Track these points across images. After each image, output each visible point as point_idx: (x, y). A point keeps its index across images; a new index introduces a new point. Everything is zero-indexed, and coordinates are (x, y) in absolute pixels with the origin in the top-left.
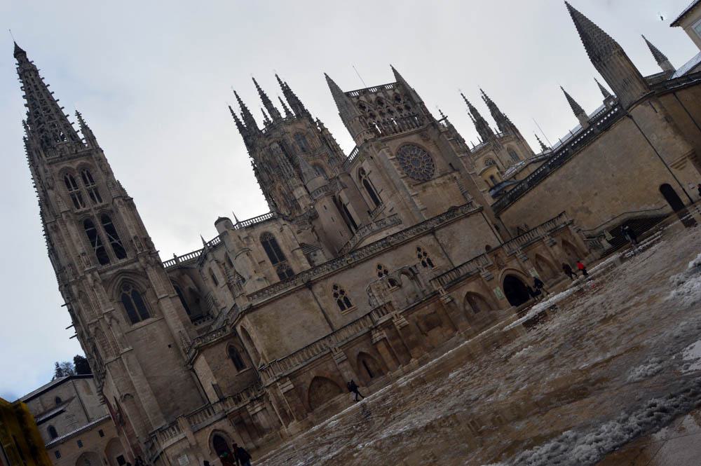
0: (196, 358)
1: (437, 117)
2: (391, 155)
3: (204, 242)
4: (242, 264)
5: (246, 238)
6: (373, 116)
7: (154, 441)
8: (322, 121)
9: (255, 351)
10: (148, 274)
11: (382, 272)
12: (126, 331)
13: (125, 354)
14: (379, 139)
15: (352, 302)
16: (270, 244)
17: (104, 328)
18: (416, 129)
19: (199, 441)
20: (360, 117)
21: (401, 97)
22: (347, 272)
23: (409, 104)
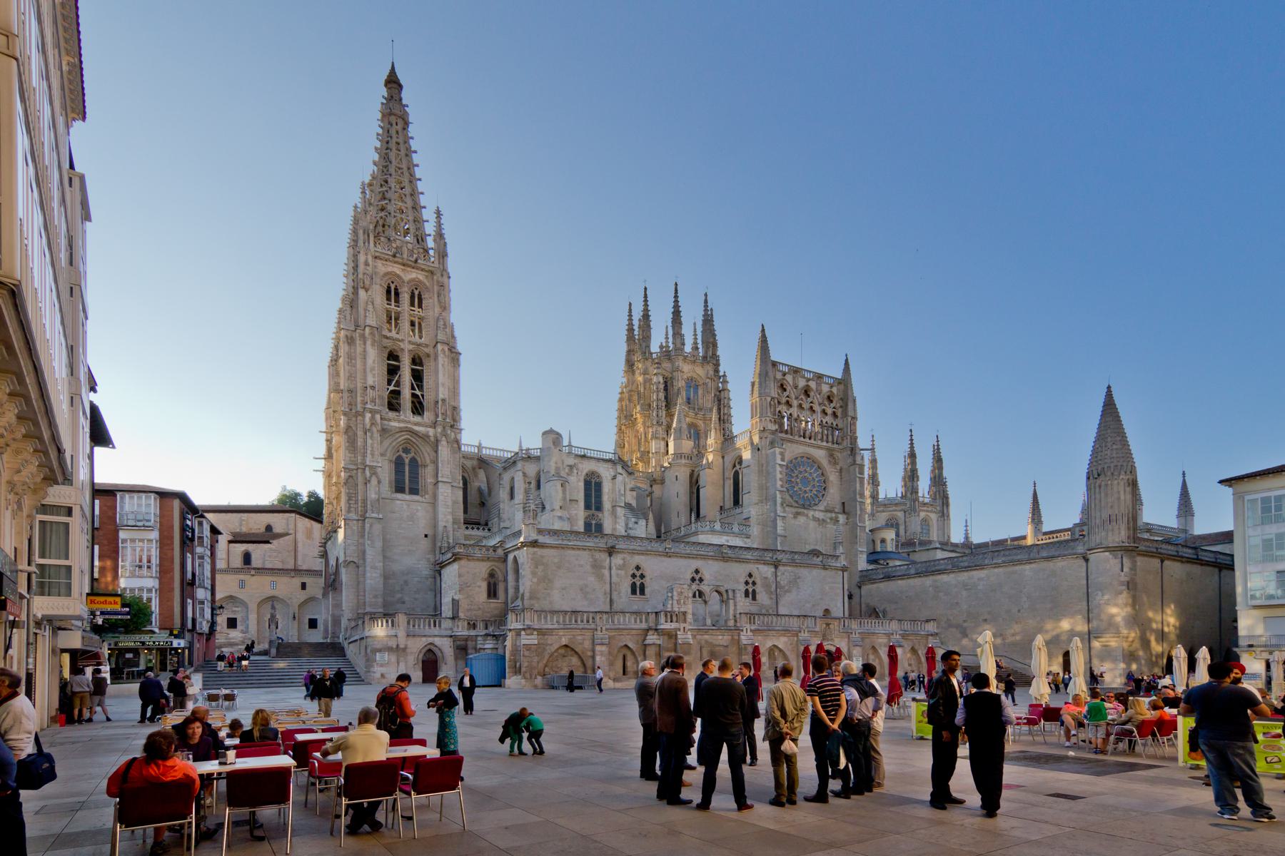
0: (449, 563)
1: (863, 442)
2: (783, 460)
3: (520, 446)
4: (552, 492)
5: (571, 467)
6: (788, 404)
7: (360, 622)
8: (728, 379)
9: (517, 589)
10: (440, 448)
11: (697, 578)
12: (383, 496)
13: (370, 520)
14: (780, 435)
15: (647, 591)
16: (593, 488)
17: (360, 480)
18: (830, 445)
19: (409, 646)
20: (773, 398)
21: (835, 400)
22: (659, 558)
23: (839, 413)
